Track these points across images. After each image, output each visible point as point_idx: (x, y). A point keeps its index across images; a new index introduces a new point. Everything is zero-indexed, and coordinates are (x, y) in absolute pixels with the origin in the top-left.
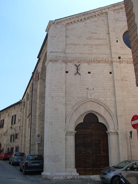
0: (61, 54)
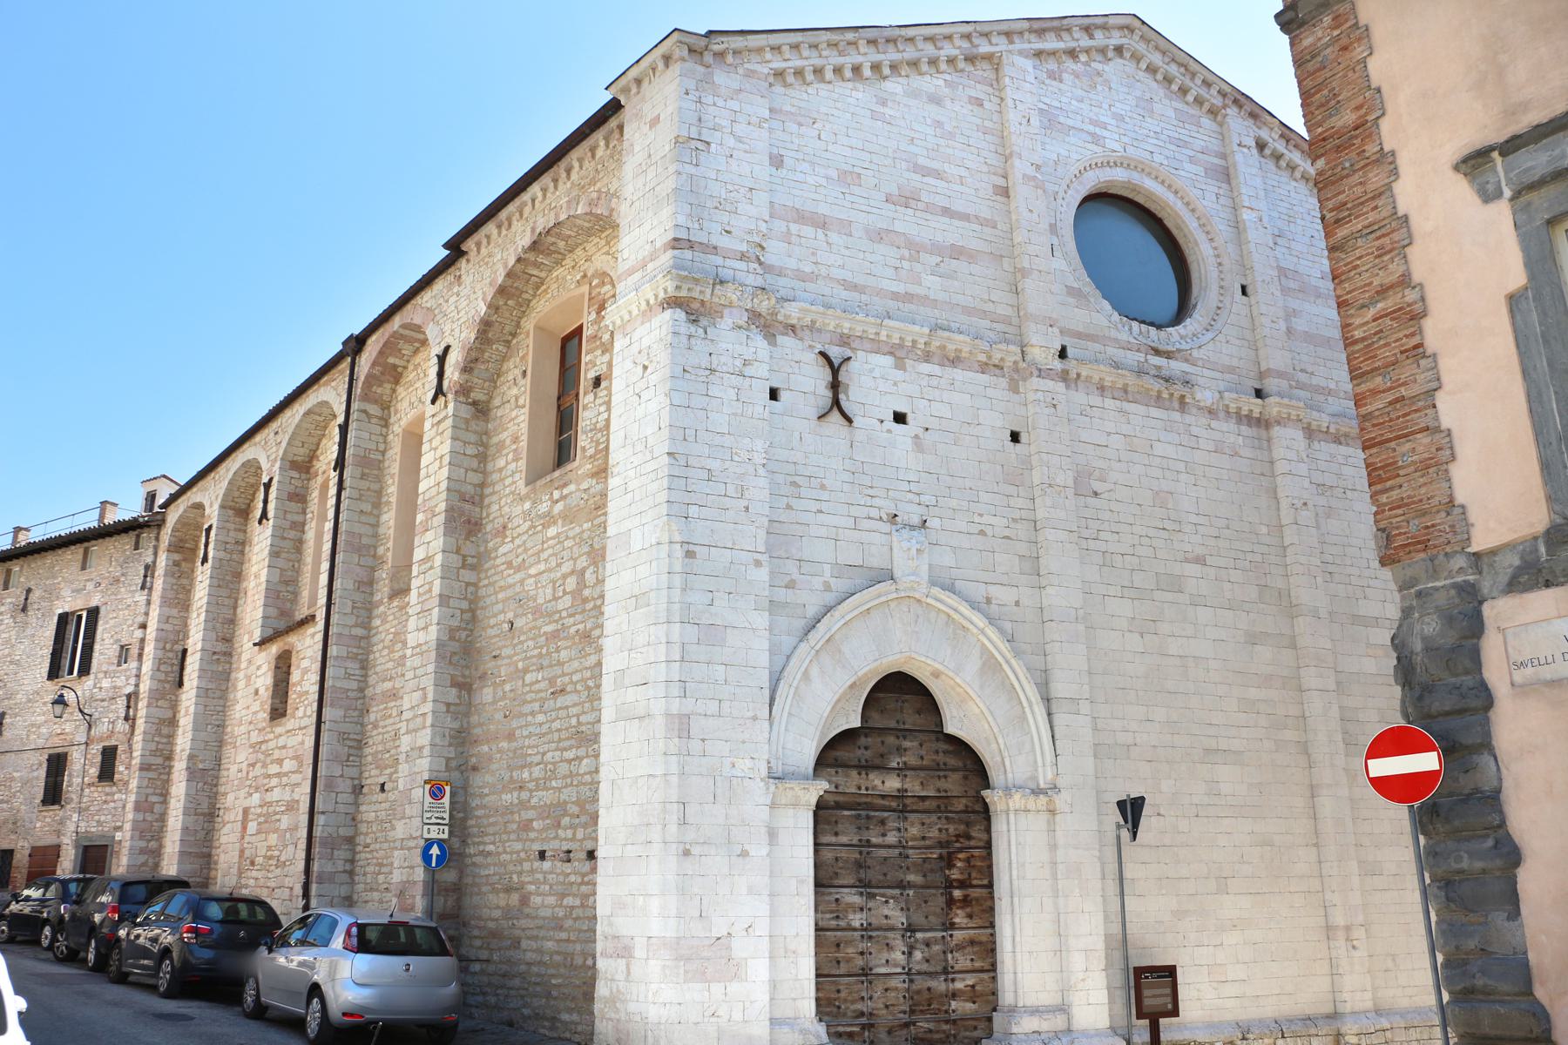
0: (742, 265)
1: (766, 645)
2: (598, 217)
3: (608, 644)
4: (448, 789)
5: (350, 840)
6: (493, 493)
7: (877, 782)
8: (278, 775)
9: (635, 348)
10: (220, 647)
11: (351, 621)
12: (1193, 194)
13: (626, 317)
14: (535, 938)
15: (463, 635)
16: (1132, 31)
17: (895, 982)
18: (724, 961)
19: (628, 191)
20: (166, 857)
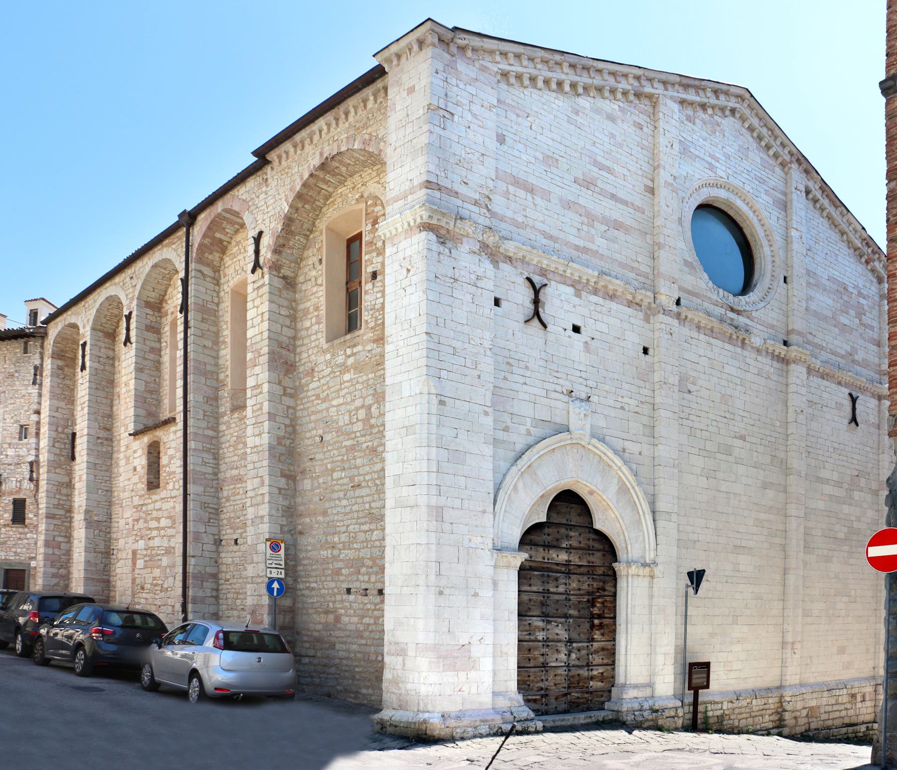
0: (473, 208)
1: (491, 467)
2: (371, 154)
3: (388, 456)
4: (283, 545)
5: (215, 576)
6: (303, 345)
7: (554, 556)
8: (157, 529)
9: (401, 255)
10: (102, 434)
11: (204, 424)
12: (765, 214)
13: (394, 232)
14: (345, 643)
15: (288, 442)
16: (743, 100)
17: (560, 671)
18: (466, 659)
19: (392, 138)
20: (74, 580)
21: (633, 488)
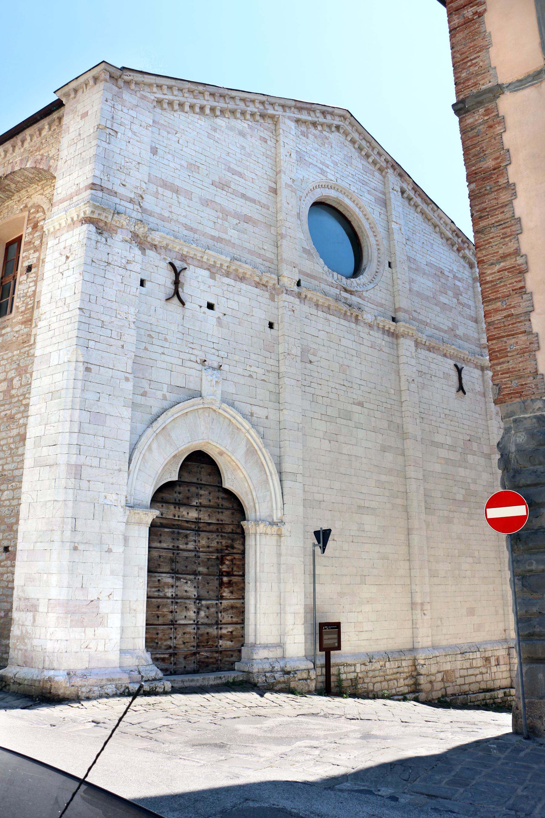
12: (369, 210)
16: (345, 119)
21: (260, 449)
